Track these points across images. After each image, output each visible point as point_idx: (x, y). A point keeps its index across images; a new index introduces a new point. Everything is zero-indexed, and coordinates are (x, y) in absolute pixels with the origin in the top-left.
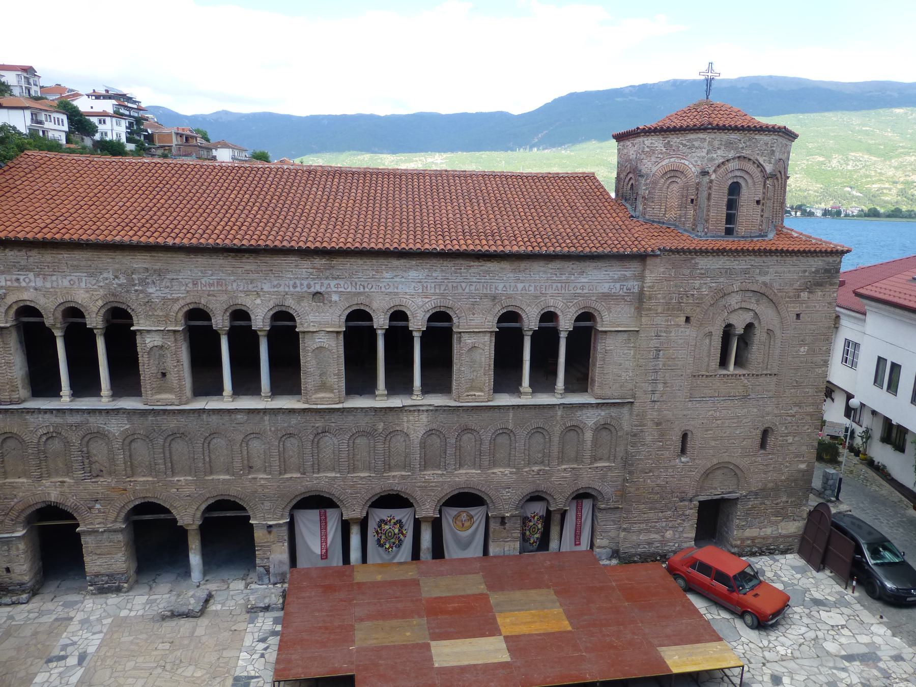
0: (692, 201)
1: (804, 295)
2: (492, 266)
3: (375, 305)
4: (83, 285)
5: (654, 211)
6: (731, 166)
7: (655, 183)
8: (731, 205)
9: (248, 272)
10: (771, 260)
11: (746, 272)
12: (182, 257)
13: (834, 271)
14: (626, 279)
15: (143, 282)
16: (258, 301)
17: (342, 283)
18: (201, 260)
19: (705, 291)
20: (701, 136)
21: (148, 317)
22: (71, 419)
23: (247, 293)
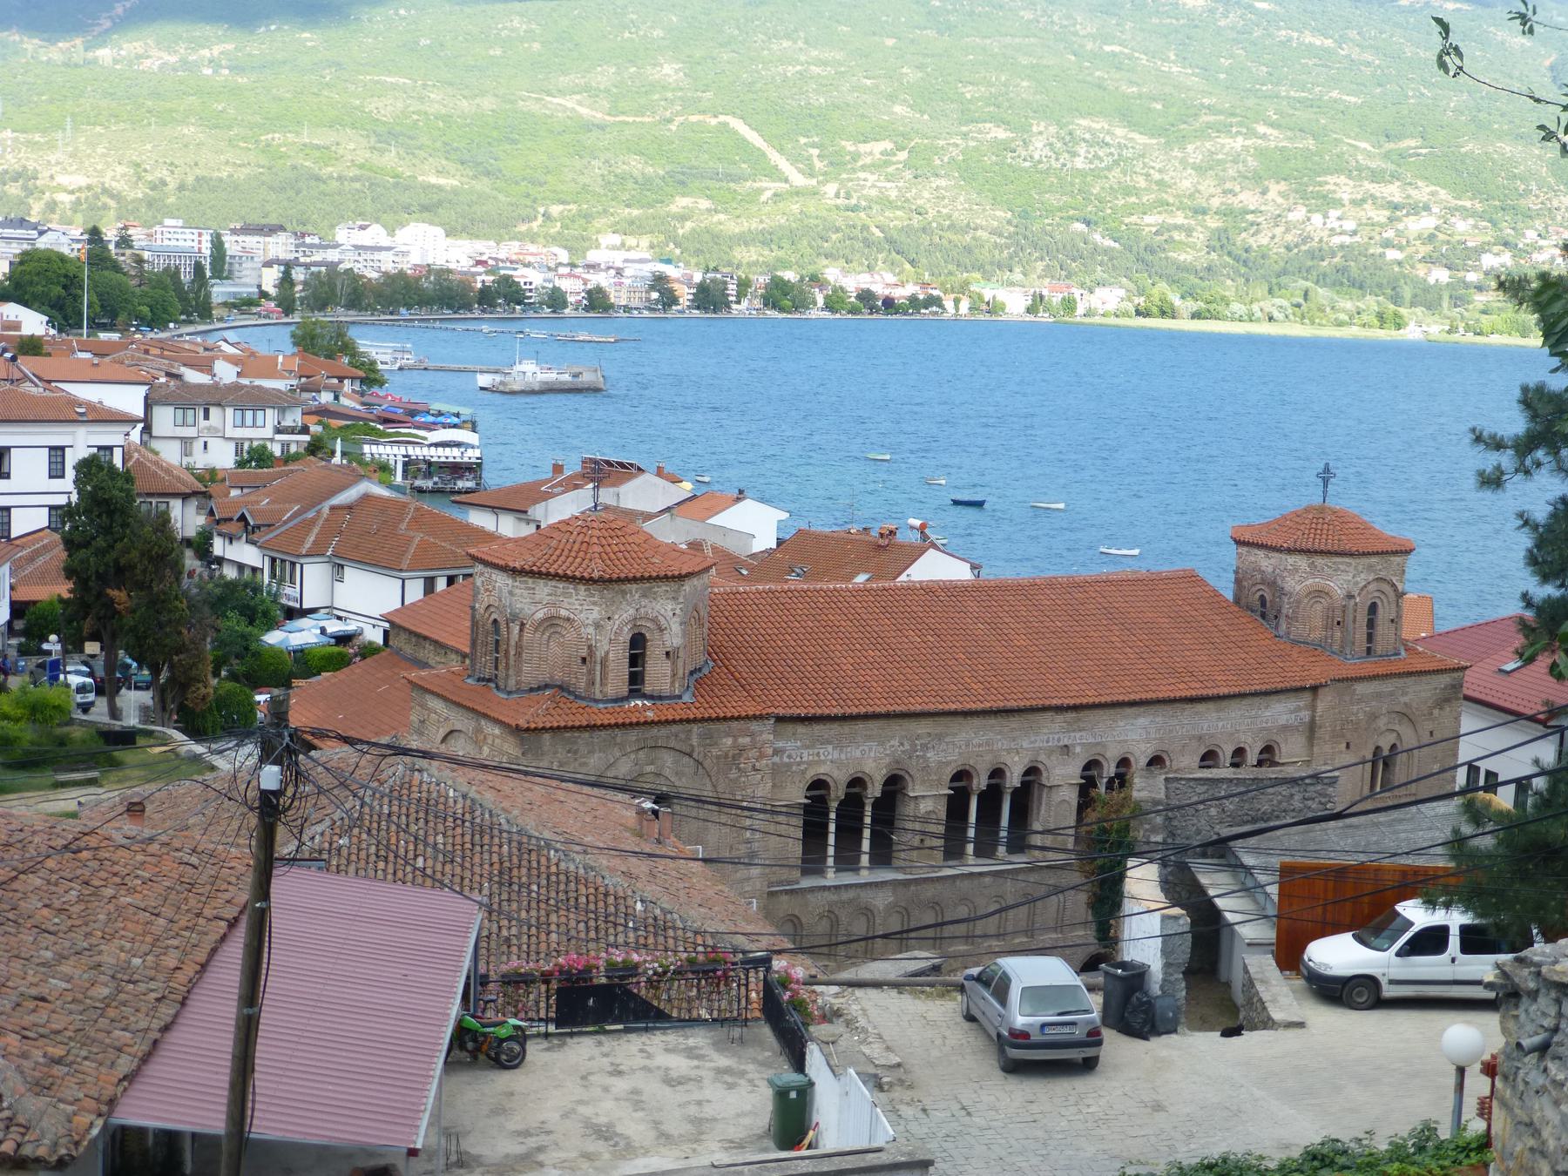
0: (1339, 623)
1: (1436, 712)
2: (1201, 707)
3: (1108, 755)
4: (872, 754)
5: (1298, 630)
6: (1372, 587)
7: (1299, 602)
8: (1371, 624)
9: (1013, 730)
10: (1410, 681)
11: (1391, 694)
12: (960, 720)
13: (1457, 687)
14: (1298, 709)
15: (925, 747)
16: (1016, 759)
17: (1083, 733)
18: (976, 722)
19: (1361, 716)
20: (1347, 560)
21: (923, 782)
22: (846, 896)
23: (1009, 751)
